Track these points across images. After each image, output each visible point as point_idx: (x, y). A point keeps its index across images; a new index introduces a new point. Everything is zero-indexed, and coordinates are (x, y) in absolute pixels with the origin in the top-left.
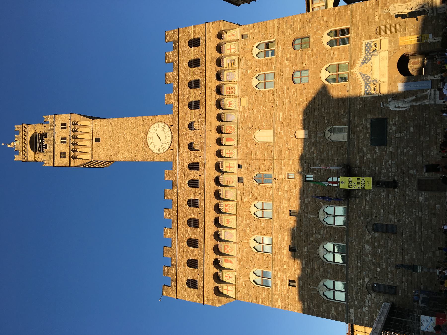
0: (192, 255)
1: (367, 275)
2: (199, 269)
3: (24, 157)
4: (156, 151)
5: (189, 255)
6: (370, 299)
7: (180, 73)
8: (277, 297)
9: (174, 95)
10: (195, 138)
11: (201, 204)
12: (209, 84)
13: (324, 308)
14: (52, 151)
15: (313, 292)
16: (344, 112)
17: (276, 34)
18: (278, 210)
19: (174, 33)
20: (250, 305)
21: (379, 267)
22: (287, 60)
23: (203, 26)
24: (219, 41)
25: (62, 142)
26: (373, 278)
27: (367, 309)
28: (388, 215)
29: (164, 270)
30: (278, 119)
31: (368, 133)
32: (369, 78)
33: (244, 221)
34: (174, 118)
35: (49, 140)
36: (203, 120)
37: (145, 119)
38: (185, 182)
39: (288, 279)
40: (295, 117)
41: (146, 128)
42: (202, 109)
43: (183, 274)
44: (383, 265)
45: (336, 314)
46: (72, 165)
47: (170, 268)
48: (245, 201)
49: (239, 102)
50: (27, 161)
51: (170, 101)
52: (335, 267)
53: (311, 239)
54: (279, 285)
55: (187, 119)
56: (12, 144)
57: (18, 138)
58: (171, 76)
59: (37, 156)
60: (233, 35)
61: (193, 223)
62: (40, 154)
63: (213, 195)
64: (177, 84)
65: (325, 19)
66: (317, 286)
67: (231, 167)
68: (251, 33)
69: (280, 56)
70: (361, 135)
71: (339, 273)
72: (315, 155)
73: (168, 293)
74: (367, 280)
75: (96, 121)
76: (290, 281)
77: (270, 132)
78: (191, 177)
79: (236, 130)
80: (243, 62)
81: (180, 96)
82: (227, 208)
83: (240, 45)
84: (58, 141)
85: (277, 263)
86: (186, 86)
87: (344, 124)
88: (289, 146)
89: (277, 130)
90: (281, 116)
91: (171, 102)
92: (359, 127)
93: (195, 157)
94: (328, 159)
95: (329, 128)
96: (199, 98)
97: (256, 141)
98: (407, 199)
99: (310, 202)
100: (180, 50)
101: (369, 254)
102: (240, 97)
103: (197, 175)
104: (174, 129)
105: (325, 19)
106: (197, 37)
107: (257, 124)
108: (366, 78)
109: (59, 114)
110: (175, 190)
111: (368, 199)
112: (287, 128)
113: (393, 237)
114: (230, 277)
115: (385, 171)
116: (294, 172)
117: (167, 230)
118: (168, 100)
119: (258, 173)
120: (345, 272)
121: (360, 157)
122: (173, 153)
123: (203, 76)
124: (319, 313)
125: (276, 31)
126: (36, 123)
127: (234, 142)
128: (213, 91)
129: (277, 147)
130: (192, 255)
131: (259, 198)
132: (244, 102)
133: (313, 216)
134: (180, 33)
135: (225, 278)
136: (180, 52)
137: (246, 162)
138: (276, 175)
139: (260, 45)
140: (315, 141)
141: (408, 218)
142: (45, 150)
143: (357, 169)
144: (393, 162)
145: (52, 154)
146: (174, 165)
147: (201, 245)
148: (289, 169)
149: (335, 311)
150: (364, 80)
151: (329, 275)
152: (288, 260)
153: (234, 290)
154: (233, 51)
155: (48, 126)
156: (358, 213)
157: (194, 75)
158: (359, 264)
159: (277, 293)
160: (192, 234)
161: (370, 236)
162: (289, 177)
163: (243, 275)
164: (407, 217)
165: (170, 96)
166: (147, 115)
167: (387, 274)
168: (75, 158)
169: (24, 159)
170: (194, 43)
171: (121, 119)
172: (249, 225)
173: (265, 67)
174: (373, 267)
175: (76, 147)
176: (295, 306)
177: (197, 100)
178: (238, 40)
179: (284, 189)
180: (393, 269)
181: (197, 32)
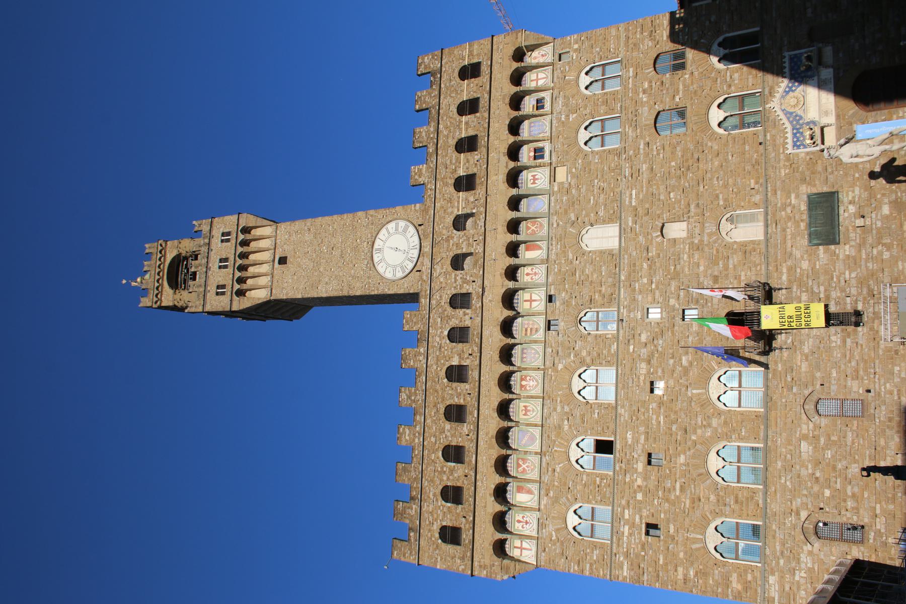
0: (451, 477)
1: (805, 506)
2: (466, 505)
3: (155, 299)
4: (389, 275)
5: (445, 478)
6: (810, 553)
7: (441, 126)
8: (622, 559)
9: (427, 168)
10: (464, 246)
11: (473, 374)
13: (716, 577)
14: (203, 285)
15: (694, 546)
16: (757, 183)
17: (622, 49)
19: (433, 57)
20: (566, 576)
21: (829, 487)
23: (486, 42)
24: (515, 65)
25: (220, 267)
26: (817, 510)
27: (805, 575)
28: (846, 381)
29: (395, 508)
30: (627, 203)
31: (802, 221)
32: (801, 118)
33: (559, 409)
34: (425, 211)
35: (200, 265)
36: (483, 209)
37: (372, 216)
38: (442, 332)
40: (662, 197)
41: (371, 233)
42: (480, 191)
43: (432, 515)
44: (836, 483)
45: (740, 587)
46: (235, 308)
47: (408, 505)
48: (560, 367)
49: (553, 174)
50: (160, 307)
52: (740, 493)
53: (694, 438)
54: (626, 534)
55: (450, 210)
56: (139, 280)
57: (149, 266)
58: (424, 134)
59: (178, 296)
62: (182, 292)
63: (496, 357)
64: (435, 146)
65: (713, 18)
66: (704, 533)
69: (630, 86)
70: (789, 224)
71: (747, 505)
72: (702, 268)
73: (404, 554)
74: (804, 514)
77: (612, 230)
78: (454, 323)
79: (546, 228)
80: (560, 101)
82: (524, 383)
84: (214, 264)
85: (623, 491)
86: (451, 150)
87: (756, 205)
88: (650, 254)
90: (634, 196)
91: (421, 180)
92: (784, 209)
94: (727, 275)
95: (728, 215)
96: (475, 170)
97: (585, 248)
98: (882, 346)
99: (691, 364)
100: (442, 86)
101: (809, 461)
102: (554, 165)
103: (467, 317)
105: (713, 18)
106: (475, 61)
107: (587, 215)
108: (794, 119)
109: (219, 216)
110: (422, 350)
111: (806, 351)
112: (646, 218)
113: (855, 425)
114: (527, 523)
115: (839, 295)
116: (659, 305)
118: (417, 177)
120: (761, 502)
121: (790, 269)
122: (421, 277)
123: (484, 128)
124: (706, 587)
125: (622, 44)
126: (180, 237)
127: (540, 252)
128: (501, 154)
130: (451, 477)
131: (588, 360)
132: (562, 174)
133: (698, 391)
135: (517, 524)
136: (443, 90)
137: (564, 290)
138: (624, 312)
139: (594, 69)
140: (701, 241)
141: (885, 384)
142: (191, 283)
143: (784, 291)
144: (853, 275)
145: (202, 289)
147: (470, 457)
148: (650, 298)
149: (738, 581)
150: (791, 122)
151: (728, 508)
152: (645, 484)
153: (534, 549)
154: (541, 83)
155: (201, 241)
156: (786, 380)
158: (788, 483)
160: (452, 436)
161: (811, 425)
163: (553, 517)
164: (882, 381)
165: (420, 170)
166: (376, 207)
167: (845, 501)
168: (241, 293)
169: (156, 302)
170: (470, 72)
171: (327, 219)
172: (569, 416)
173: (603, 107)
174: (816, 488)
175: (244, 274)
176: (658, 576)
177: (470, 172)
178: (552, 64)
180: (856, 490)
181: (475, 53)
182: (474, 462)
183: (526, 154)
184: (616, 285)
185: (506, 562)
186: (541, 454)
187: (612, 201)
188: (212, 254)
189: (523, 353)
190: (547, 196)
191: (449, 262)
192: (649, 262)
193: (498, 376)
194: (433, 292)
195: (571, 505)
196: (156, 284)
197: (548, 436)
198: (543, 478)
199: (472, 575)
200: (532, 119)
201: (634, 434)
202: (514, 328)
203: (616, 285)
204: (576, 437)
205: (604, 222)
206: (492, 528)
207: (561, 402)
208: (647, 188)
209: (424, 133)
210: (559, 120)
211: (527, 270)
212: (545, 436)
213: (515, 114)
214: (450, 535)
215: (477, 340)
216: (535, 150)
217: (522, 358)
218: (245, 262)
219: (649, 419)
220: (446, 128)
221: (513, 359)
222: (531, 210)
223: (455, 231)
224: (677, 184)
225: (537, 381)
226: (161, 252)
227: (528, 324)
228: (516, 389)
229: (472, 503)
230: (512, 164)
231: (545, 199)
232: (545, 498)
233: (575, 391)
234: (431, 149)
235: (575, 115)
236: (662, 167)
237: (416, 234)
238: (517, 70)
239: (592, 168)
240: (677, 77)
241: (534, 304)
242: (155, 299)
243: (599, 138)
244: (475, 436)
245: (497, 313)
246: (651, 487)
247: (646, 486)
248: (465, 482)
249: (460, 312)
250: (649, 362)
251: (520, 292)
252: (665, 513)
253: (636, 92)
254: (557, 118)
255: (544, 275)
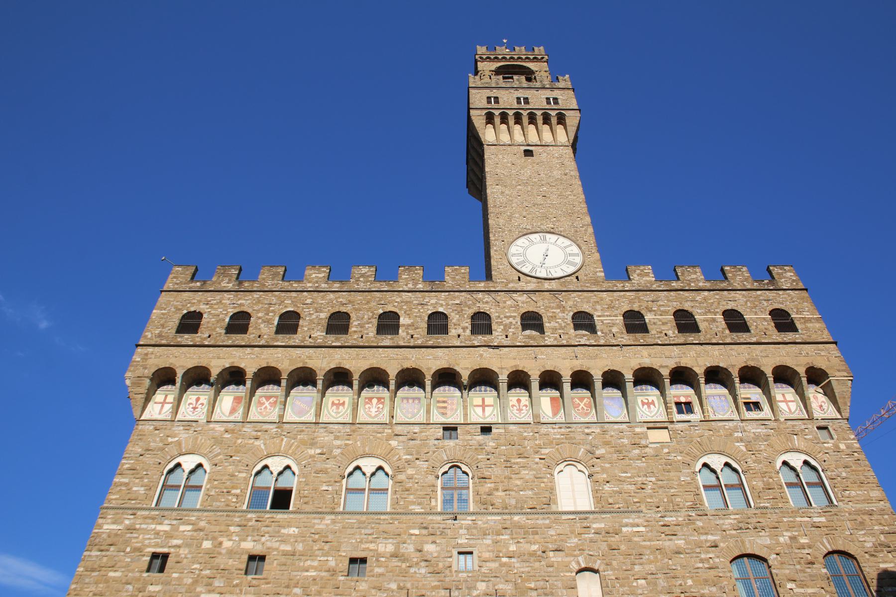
3: (484, 57)
4: (513, 249)
5: (260, 315)
7: (706, 293)
8: (127, 522)
9: (652, 283)
10: (553, 324)
11: (387, 340)
12: (693, 351)
18: (365, 528)
20: (118, 453)
22: (790, 538)
23: (826, 336)
29: (231, 266)
30: (625, 521)
33: (338, 443)
34: (596, 282)
36: (602, 342)
38: (442, 305)
39: (172, 550)
42: (627, 338)
43: (217, 303)
46: (472, 112)
47: (234, 279)
49: (658, 425)
50: (476, 61)
51: (635, 276)
54: (159, 528)
57: (520, 50)
58: (694, 276)
60: (821, 406)
61: (338, 323)
63: (407, 365)
64: (679, 288)
67: (484, 410)
68: (837, 447)
69: (798, 519)
75: (570, 151)
76: (165, 556)
77: (585, 503)
78: (454, 318)
79: (582, 420)
81: (653, 295)
82: (375, 401)
83: (800, 422)
84: (521, 94)
86: (677, 306)
88: (551, 554)
89: (595, 520)
90: (636, 529)
91: (635, 277)
93: (505, 326)
96: (653, 332)
100: (759, 293)
102: (670, 426)
104: (570, 283)
106: (799, 326)
107: (604, 470)
112: (604, 546)
114: (194, 408)
116: (477, 568)
117: (324, 272)
119: (471, 475)
122: (512, 281)
125: (859, 506)
128: (677, 360)
129: (547, 522)
130: (260, 321)
131: (401, 477)
134: (797, 292)
136: (754, 293)
138: (467, 521)
145: (494, 85)
146: (482, 284)
147: (282, 340)
148: (487, 555)
152: (224, 551)
154: (783, 406)
157: (707, 321)
159: (139, 521)
162: (462, 557)
163: (197, 438)
165: (647, 275)
166: (597, 233)
168: (490, 118)
169: (481, 58)
170: (783, 321)
172: (326, 455)
173: (760, 485)
175: (511, 121)
177: (649, 327)
178: (811, 418)
179: (427, 543)
181: (809, 325)
182: (276, 344)
183: (683, 393)
184: (506, 510)
185: (147, 382)
186: (281, 423)
187: (626, 502)
188: (534, 92)
189: (414, 399)
190: (627, 420)
191: (531, 309)
192: (539, 553)
193: (383, 367)
194: (493, 294)
195: (209, 460)
196: (500, 57)
197: (303, 431)
198: (248, 425)
199: (137, 346)
200: (730, 398)
201: (295, 536)
202: (447, 388)
203: (506, 510)
204: (298, 464)
205: (595, 491)
206: (190, 364)
207: (346, 445)
208: (650, 547)
209: (695, 276)
210: (735, 429)
211: (525, 400)
212: (303, 427)
213: (735, 373)
214: (190, 323)
215: (430, 343)
216: (688, 404)
217: (407, 399)
218: (525, 120)
219: (312, 556)
220: (705, 299)
221: (406, 388)
222: (606, 402)
223: (572, 314)
224: (659, 588)
225: (376, 416)
226: (535, 58)
227: (453, 404)
228: (366, 393)
229: (225, 343)
230: (665, 372)
231: (623, 416)
232: (223, 429)
233: (360, 462)
234: (674, 284)
235: (744, 449)
236: (683, 566)
237: (566, 274)
238: (796, 373)
239: (672, 474)
240: (824, 584)
241: (479, 410)
242: (484, 57)
243: (715, 483)
244: (308, 344)
245: (465, 364)
246: (217, 560)
247: (220, 553)
248: (252, 336)
249: (467, 324)
250: (394, 555)
251: (495, 393)
252: (179, 578)
253: (790, 528)
254: (736, 427)
255: (518, 420)
